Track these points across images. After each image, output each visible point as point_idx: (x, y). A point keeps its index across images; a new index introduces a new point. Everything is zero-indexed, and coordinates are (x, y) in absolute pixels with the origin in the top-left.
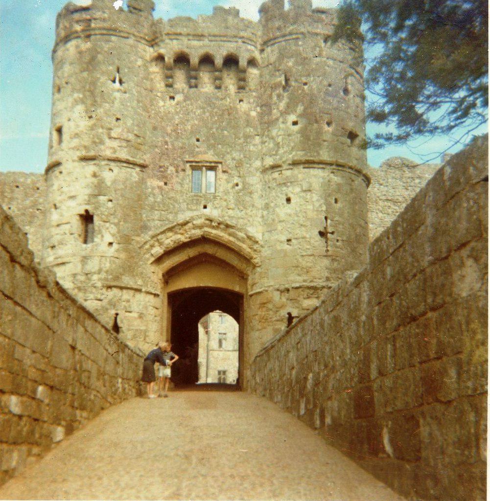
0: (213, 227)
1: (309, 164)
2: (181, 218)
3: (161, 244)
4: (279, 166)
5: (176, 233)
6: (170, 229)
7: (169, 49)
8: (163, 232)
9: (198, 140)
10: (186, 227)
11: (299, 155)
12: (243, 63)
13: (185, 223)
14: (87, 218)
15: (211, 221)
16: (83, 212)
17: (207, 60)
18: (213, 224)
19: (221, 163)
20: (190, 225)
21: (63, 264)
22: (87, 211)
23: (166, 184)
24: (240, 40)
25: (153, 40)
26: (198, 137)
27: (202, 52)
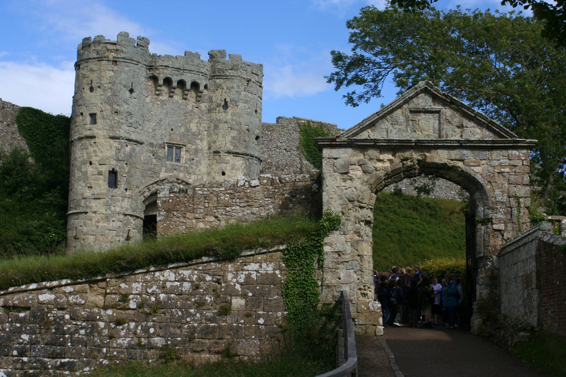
0: (179, 183)
1: (236, 154)
2: (163, 175)
3: (149, 190)
4: (219, 152)
5: (158, 185)
6: (156, 183)
7: (161, 75)
8: (152, 184)
9: (172, 130)
10: (164, 182)
11: (231, 148)
12: (202, 88)
13: (164, 180)
14: (113, 173)
15: (178, 179)
16: (111, 170)
17: (182, 84)
18: (179, 181)
19: (185, 146)
20: (166, 181)
21: (99, 199)
22: (113, 169)
23: (153, 155)
24: (201, 74)
25: (150, 66)
26: (172, 128)
27: (179, 78)
